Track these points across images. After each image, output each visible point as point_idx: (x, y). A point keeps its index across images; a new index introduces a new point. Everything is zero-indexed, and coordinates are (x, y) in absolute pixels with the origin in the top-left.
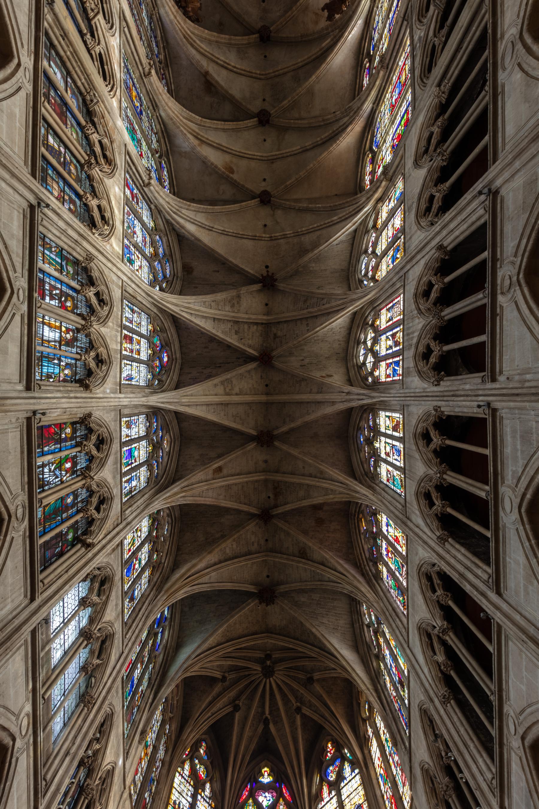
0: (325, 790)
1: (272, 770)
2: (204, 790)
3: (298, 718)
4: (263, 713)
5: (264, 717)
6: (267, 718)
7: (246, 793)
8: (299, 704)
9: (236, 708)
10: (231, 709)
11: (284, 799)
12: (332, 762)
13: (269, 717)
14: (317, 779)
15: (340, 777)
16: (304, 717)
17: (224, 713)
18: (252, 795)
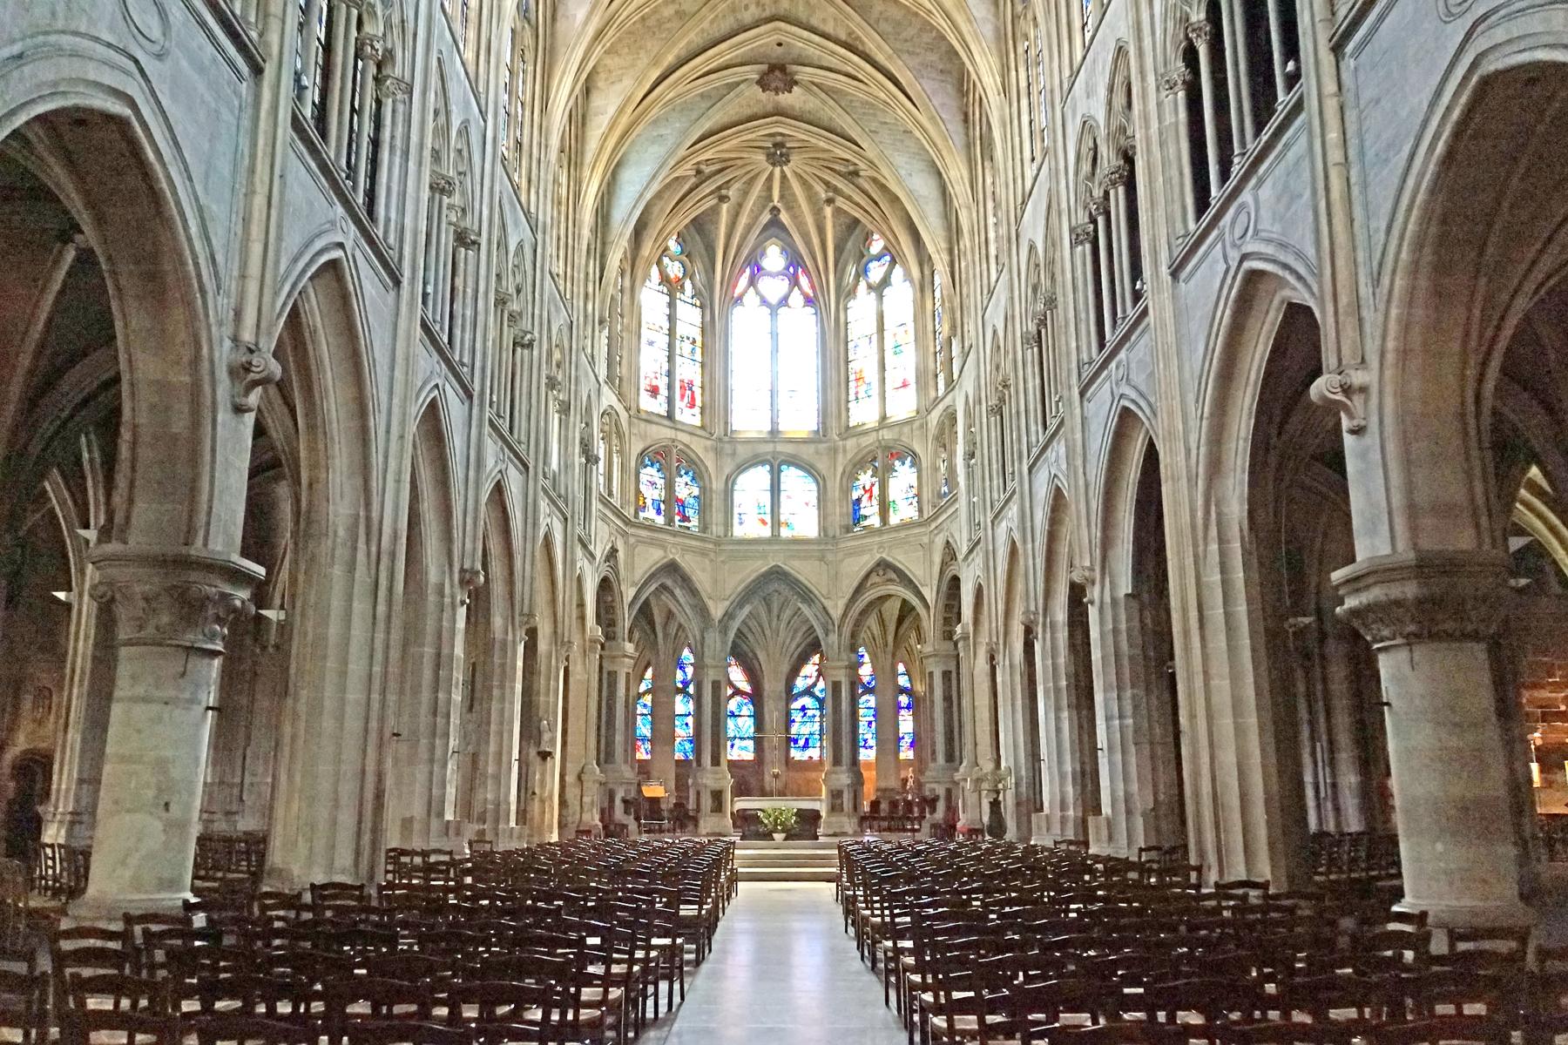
0: (862, 285)
1: (783, 250)
2: (682, 290)
3: (828, 211)
4: (770, 198)
6: (775, 208)
7: (743, 281)
9: (723, 199)
10: (715, 201)
12: (878, 258)
13: (779, 205)
14: (851, 270)
15: (885, 282)
16: (838, 212)
18: (752, 282)
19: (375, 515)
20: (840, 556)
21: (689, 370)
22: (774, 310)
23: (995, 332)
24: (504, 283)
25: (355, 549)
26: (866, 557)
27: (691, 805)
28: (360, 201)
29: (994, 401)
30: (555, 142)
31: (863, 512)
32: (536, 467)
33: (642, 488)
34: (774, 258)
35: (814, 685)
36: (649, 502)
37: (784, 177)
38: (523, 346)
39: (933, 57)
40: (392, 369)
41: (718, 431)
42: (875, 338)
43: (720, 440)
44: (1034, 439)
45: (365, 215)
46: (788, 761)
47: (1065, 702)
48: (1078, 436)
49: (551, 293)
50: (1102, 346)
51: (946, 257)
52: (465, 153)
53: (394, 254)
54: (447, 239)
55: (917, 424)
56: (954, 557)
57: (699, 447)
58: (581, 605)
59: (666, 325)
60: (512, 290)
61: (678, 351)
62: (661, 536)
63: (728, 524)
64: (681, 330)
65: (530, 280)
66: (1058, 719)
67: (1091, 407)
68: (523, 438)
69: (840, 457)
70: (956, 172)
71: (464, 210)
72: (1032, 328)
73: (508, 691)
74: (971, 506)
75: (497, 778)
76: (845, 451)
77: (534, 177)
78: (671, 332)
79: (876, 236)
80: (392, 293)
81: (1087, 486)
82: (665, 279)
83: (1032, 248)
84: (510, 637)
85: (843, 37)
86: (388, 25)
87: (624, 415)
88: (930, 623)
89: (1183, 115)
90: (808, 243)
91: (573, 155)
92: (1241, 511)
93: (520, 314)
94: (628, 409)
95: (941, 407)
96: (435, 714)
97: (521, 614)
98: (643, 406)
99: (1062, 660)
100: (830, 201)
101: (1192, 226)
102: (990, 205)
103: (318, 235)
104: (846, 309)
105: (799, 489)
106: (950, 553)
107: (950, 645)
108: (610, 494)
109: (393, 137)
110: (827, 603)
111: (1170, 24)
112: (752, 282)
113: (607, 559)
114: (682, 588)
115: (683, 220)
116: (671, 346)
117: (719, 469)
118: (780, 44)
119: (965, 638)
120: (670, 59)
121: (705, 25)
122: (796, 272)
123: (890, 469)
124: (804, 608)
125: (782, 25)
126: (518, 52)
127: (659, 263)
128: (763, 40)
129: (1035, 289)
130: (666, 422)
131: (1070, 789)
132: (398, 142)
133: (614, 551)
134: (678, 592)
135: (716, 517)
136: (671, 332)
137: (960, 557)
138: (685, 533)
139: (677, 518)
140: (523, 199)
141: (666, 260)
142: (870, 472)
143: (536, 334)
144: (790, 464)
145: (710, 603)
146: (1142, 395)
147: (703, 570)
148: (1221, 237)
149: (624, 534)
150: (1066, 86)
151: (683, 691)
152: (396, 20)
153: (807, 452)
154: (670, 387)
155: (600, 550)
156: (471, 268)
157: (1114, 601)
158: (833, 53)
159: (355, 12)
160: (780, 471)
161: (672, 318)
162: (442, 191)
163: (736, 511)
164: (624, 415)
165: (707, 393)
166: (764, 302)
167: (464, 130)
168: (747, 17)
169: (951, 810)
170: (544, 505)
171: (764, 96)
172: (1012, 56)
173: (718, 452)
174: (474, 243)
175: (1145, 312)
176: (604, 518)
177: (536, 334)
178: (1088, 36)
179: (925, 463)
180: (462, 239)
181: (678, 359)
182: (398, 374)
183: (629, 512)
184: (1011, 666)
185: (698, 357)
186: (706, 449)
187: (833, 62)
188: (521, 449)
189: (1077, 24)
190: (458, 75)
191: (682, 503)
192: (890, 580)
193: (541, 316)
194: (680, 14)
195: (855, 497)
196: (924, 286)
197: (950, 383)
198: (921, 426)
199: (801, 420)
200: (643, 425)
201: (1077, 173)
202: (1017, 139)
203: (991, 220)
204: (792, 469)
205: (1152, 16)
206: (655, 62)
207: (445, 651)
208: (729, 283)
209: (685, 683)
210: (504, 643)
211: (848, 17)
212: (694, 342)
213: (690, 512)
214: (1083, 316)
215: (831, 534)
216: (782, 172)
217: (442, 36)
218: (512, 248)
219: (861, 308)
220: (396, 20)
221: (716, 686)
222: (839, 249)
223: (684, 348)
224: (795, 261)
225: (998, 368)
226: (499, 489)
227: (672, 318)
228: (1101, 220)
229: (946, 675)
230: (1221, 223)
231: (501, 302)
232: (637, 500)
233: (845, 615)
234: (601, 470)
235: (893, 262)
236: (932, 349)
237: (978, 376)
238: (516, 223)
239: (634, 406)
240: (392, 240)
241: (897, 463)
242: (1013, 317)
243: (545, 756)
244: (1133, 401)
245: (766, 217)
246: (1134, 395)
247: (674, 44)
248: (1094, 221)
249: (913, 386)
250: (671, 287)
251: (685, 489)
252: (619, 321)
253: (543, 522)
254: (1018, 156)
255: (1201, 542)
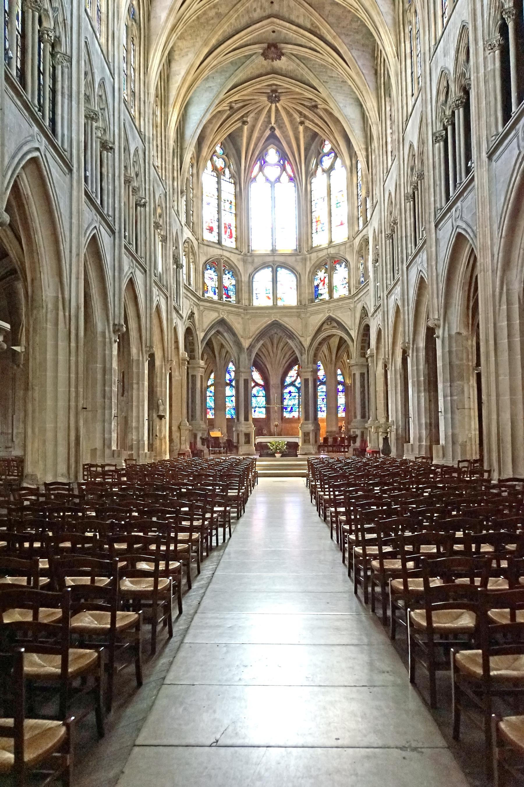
1: (277, 151)
2: (224, 175)
3: (301, 128)
4: (269, 122)
5: (270, 125)
8: (302, 119)
9: (244, 123)
10: (240, 124)
11: (286, 172)
12: (328, 154)
14: (314, 161)
15: (332, 168)
17: (234, 128)
18: (261, 169)
19: (67, 296)
20: (308, 315)
21: (229, 218)
22: (272, 185)
23: (390, 194)
24: (129, 171)
25: (57, 314)
26: (321, 315)
27: (235, 440)
28: (47, 124)
29: (389, 232)
30: (152, 91)
31: (320, 292)
32: (150, 270)
33: (206, 281)
34: (272, 156)
35: (295, 381)
36: (210, 288)
37: (277, 110)
38: (141, 206)
39: (358, 37)
40: (71, 218)
41: (245, 250)
42: (326, 199)
43: (245, 255)
44: (409, 251)
45: (50, 132)
46: (282, 418)
47: (422, 388)
48: (434, 249)
49: (154, 177)
50: (448, 199)
51: (364, 153)
52: (104, 97)
53: (67, 154)
54: (96, 146)
55: (348, 245)
56: (367, 315)
57: (235, 259)
58: (177, 342)
59: (216, 194)
60: (133, 175)
61: (223, 208)
62: (216, 306)
63: (250, 300)
64: (224, 196)
65: (142, 170)
66: (419, 397)
67: (441, 233)
68: (143, 255)
69: (308, 263)
70: (370, 104)
71: (105, 130)
72: (410, 191)
73: (141, 385)
74: (376, 288)
75: (137, 428)
76: (310, 259)
77: (142, 111)
78: (219, 198)
79: (327, 142)
80: (68, 176)
81: (437, 275)
82: (215, 169)
83: (411, 146)
84: (141, 359)
85: (309, 26)
86: (56, 22)
87: (195, 243)
88: (354, 348)
89: (498, 64)
90: (290, 147)
91: (163, 98)
92: (520, 287)
93: (139, 188)
94: (197, 240)
95: (361, 235)
96: (104, 398)
97: (146, 346)
98: (205, 238)
99: (421, 367)
100: (302, 123)
101: (500, 129)
102: (388, 122)
103: (25, 143)
104: (311, 183)
105: (287, 280)
106: (364, 312)
107: (364, 359)
108: (190, 284)
109: (63, 87)
110: (302, 339)
111: (492, 11)
112: (261, 169)
113: (189, 318)
114: (227, 332)
115: (223, 135)
116: (219, 205)
117: (245, 271)
118: (274, 32)
119: (372, 356)
120: (213, 42)
121: (233, 20)
122: (284, 162)
123: (334, 269)
124: (290, 341)
125: (275, 20)
126: (130, 39)
127: (211, 159)
128: (263, 29)
129: (412, 169)
130: (218, 246)
131: (424, 432)
132: (66, 91)
133: (192, 314)
134: (225, 334)
135: (245, 296)
136: (219, 198)
137: (370, 315)
138: (228, 304)
139: (224, 296)
140: (137, 124)
141: (215, 158)
142: (323, 271)
143: (147, 199)
144: (282, 267)
145: (242, 340)
146: (468, 225)
147: (239, 323)
148: (516, 135)
149: (197, 305)
150: (432, 51)
151: (230, 384)
152: (60, 19)
153: (291, 261)
154: (219, 227)
155: (185, 313)
156: (110, 163)
157: (450, 335)
158: (303, 36)
159: (37, 14)
160: (277, 271)
161: (219, 190)
162: (92, 119)
163: (255, 292)
164: (195, 243)
165: (239, 230)
166: (267, 180)
167: (102, 84)
168: (256, 15)
169: (364, 442)
170: (155, 290)
171: (265, 63)
172: (402, 34)
173: (245, 261)
174: (111, 148)
175: (472, 179)
176: (187, 297)
177: (147, 199)
178: (445, 20)
179: (352, 265)
180: (105, 146)
181: (223, 212)
182: (74, 220)
183: (200, 294)
184: (395, 370)
185: (233, 211)
186: (238, 260)
187: (303, 41)
188: (142, 261)
189: (439, 13)
190: (97, 52)
191: (226, 289)
192: (334, 327)
193: (149, 189)
194: (219, 15)
195: (316, 284)
196: (353, 169)
197: (366, 223)
198: (350, 246)
199: (287, 244)
200: (205, 247)
201: (437, 102)
202: (404, 83)
203: (389, 131)
204: (283, 269)
205: (482, 6)
206: (206, 44)
207: (108, 366)
208: (249, 169)
209: (231, 381)
210: (139, 360)
211: (311, 14)
212: (231, 203)
213: (231, 293)
214: (438, 183)
215: (303, 303)
216: (276, 106)
217: (86, 28)
218: (132, 152)
219: (319, 182)
220: (60, 19)
221: (246, 382)
222: (307, 150)
223: (225, 206)
224: (283, 156)
225: (391, 213)
226: (131, 282)
227: (219, 190)
228: (449, 128)
229: (362, 375)
230: (517, 127)
231: (128, 181)
232: (204, 287)
233: (311, 344)
234: (185, 272)
235: (336, 157)
236: (356, 205)
237: (381, 219)
238: (134, 138)
239: (200, 238)
240: (66, 146)
241: (338, 266)
242: (400, 185)
243: (161, 417)
244: (464, 230)
245: (268, 133)
246: (464, 226)
247: (216, 33)
248: (446, 129)
249: (346, 225)
250: (218, 173)
251: (228, 281)
252: (190, 190)
253: (155, 299)
254: (404, 94)
255: (497, 304)
